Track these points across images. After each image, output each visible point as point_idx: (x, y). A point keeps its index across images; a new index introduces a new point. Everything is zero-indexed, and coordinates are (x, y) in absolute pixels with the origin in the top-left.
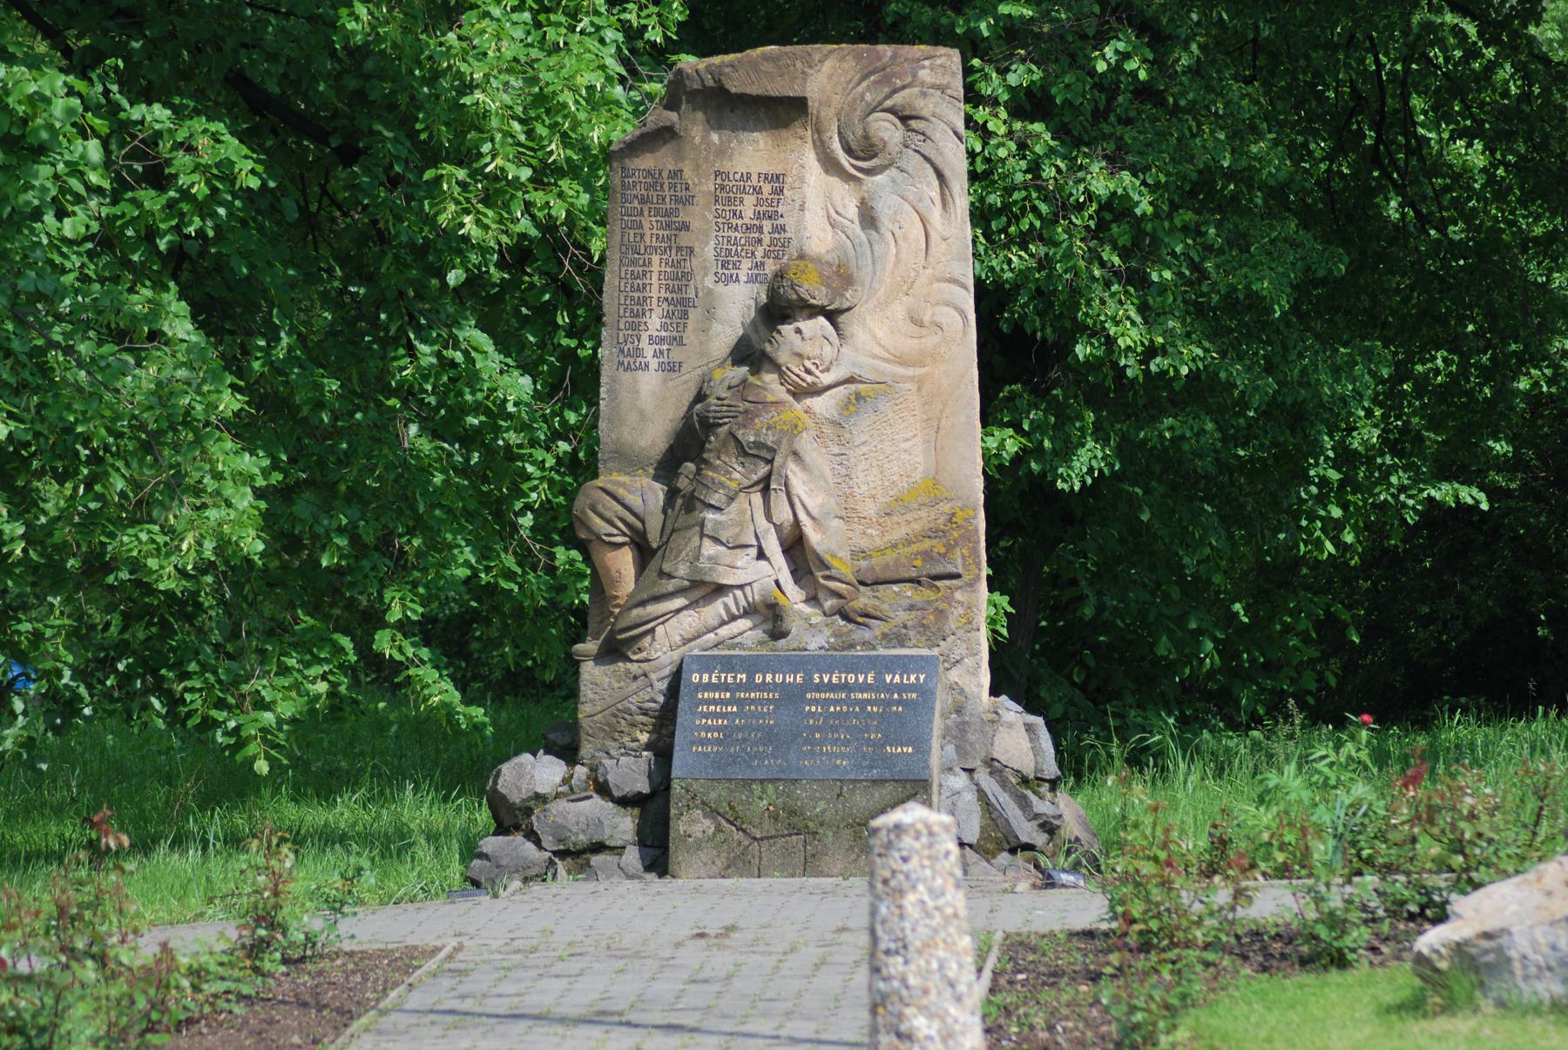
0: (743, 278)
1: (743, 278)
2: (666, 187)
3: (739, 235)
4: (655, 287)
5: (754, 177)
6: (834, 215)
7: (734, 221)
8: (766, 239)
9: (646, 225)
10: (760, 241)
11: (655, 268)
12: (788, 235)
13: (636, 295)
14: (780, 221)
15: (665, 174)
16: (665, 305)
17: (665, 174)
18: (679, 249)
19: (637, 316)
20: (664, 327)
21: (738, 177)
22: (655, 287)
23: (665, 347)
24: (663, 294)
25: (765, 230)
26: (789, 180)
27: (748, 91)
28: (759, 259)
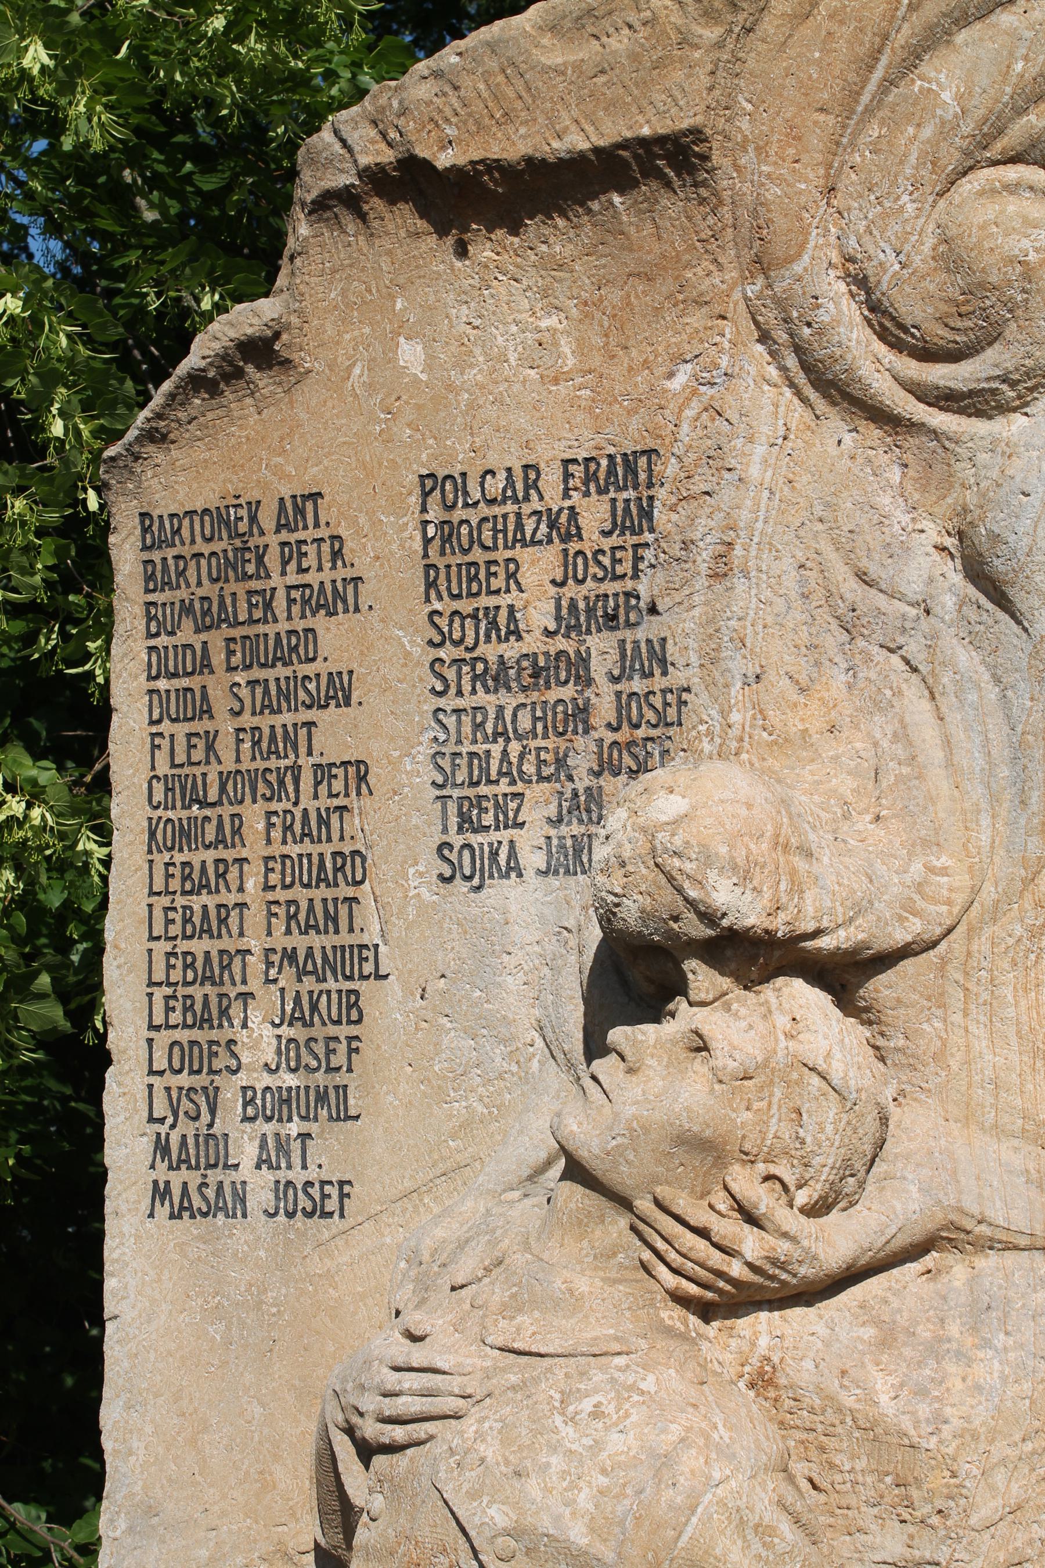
0: (532, 859)
1: (532, 859)
2: (272, 560)
3: (509, 701)
4: (255, 916)
5: (551, 480)
6: (851, 588)
7: (490, 651)
8: (604, 708)
9: (221, 702)
10: (581, 713)
11: (254, 848)
12: (677, 677)
13: (199, 946)
14: (648, 630)
15: (267, 519)
16: (287, 978)
17: (267, 519)
18: (323, 772)
19: (204, 1022)
20: (286, 1047)
21: (496, 486)
22: (255, 916)
23: (294, 1128)
24: (280, 940)
25: (598, 669)
26: (671, 469)
27: (495, 151)
28: (583, 781)
